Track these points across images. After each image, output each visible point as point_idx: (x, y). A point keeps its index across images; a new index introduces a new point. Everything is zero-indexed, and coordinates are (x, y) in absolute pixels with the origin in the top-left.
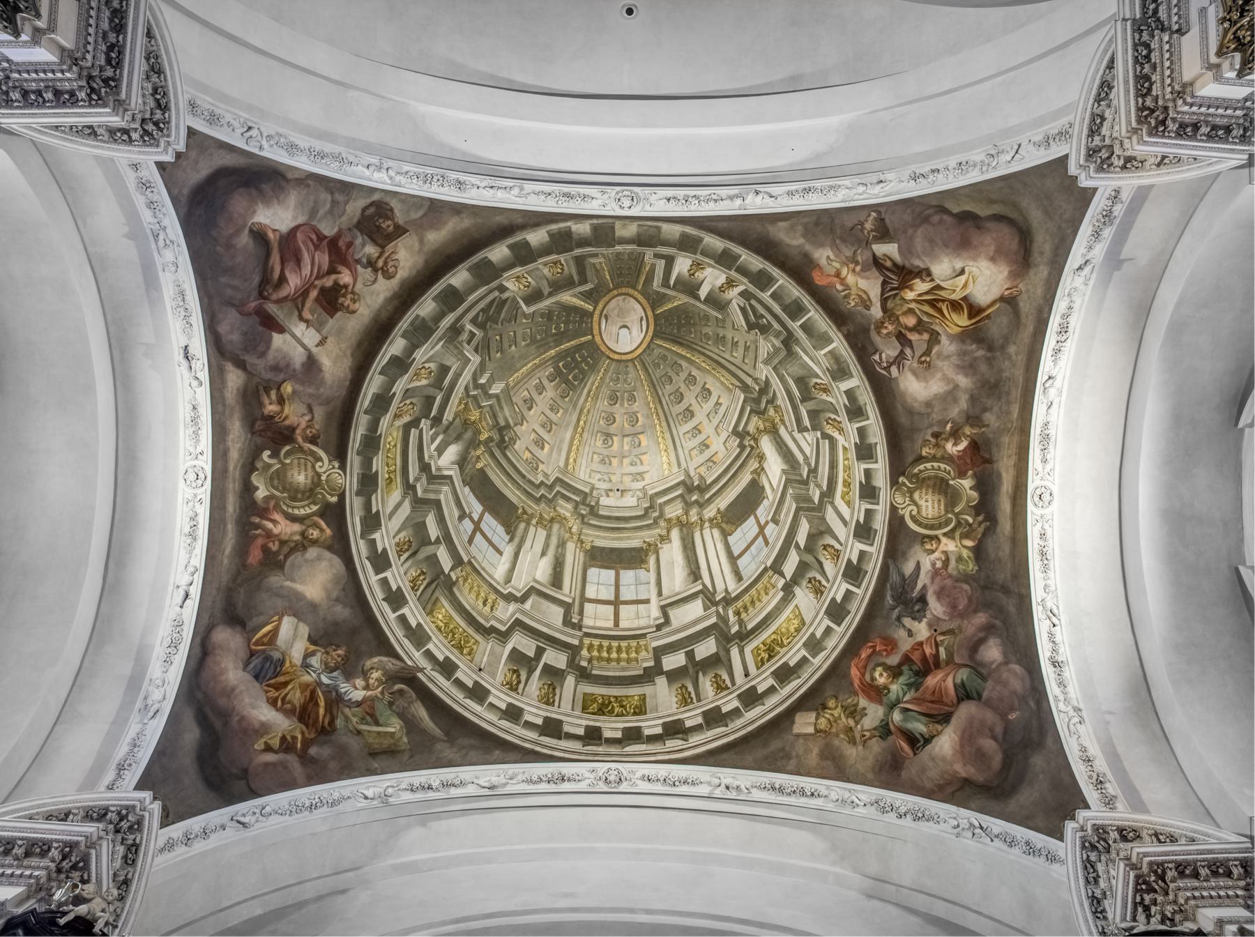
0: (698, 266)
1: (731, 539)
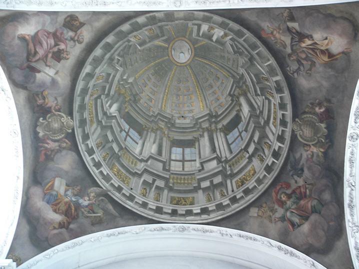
0: (211, 28)
1: (228, 137)
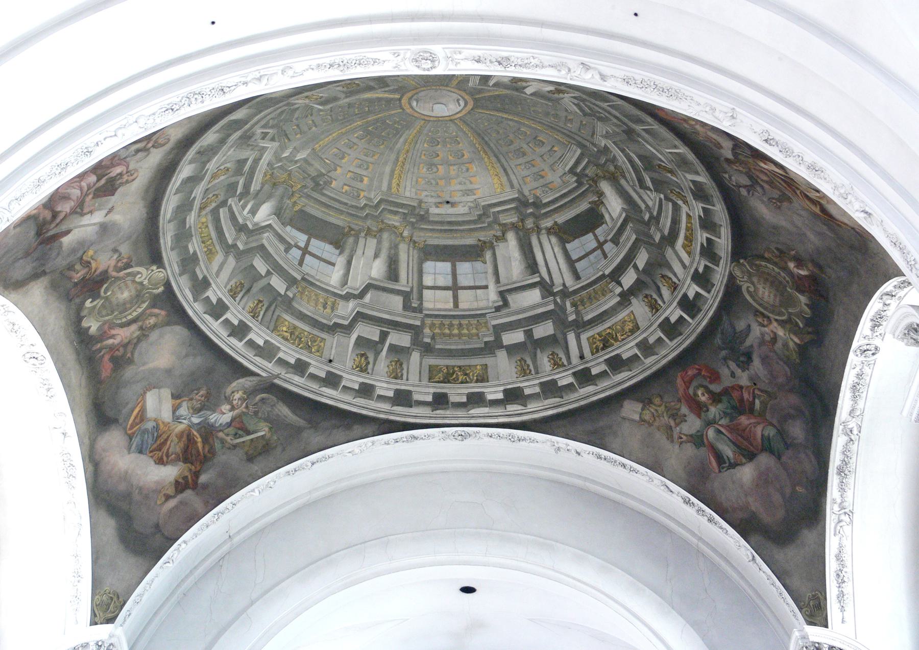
1: (569, 246)
